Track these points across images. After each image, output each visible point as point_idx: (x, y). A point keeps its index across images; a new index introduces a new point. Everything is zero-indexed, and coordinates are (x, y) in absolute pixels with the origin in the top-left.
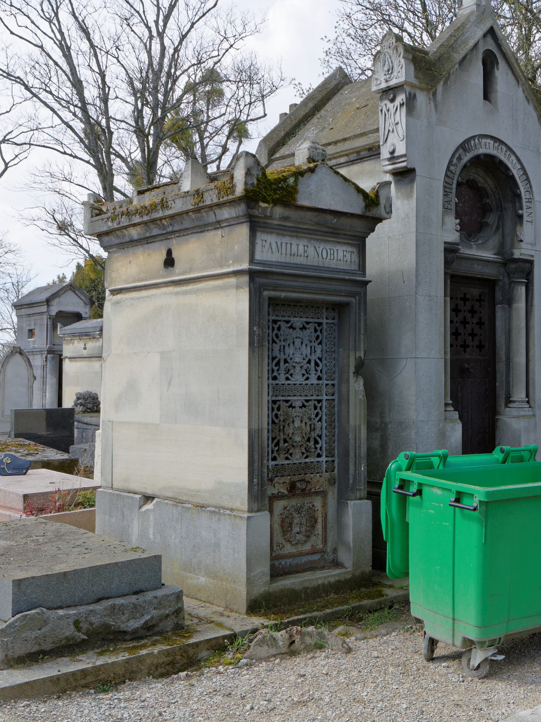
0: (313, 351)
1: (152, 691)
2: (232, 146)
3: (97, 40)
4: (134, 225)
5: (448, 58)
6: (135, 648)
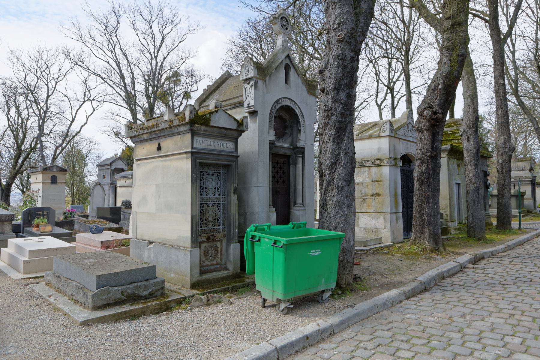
0: (217, 184)
1: (152, 320)
2: (184, 102)
3: (130, 60)
4: (145, 133)
5: (271, 67)
6: (145, 302)
